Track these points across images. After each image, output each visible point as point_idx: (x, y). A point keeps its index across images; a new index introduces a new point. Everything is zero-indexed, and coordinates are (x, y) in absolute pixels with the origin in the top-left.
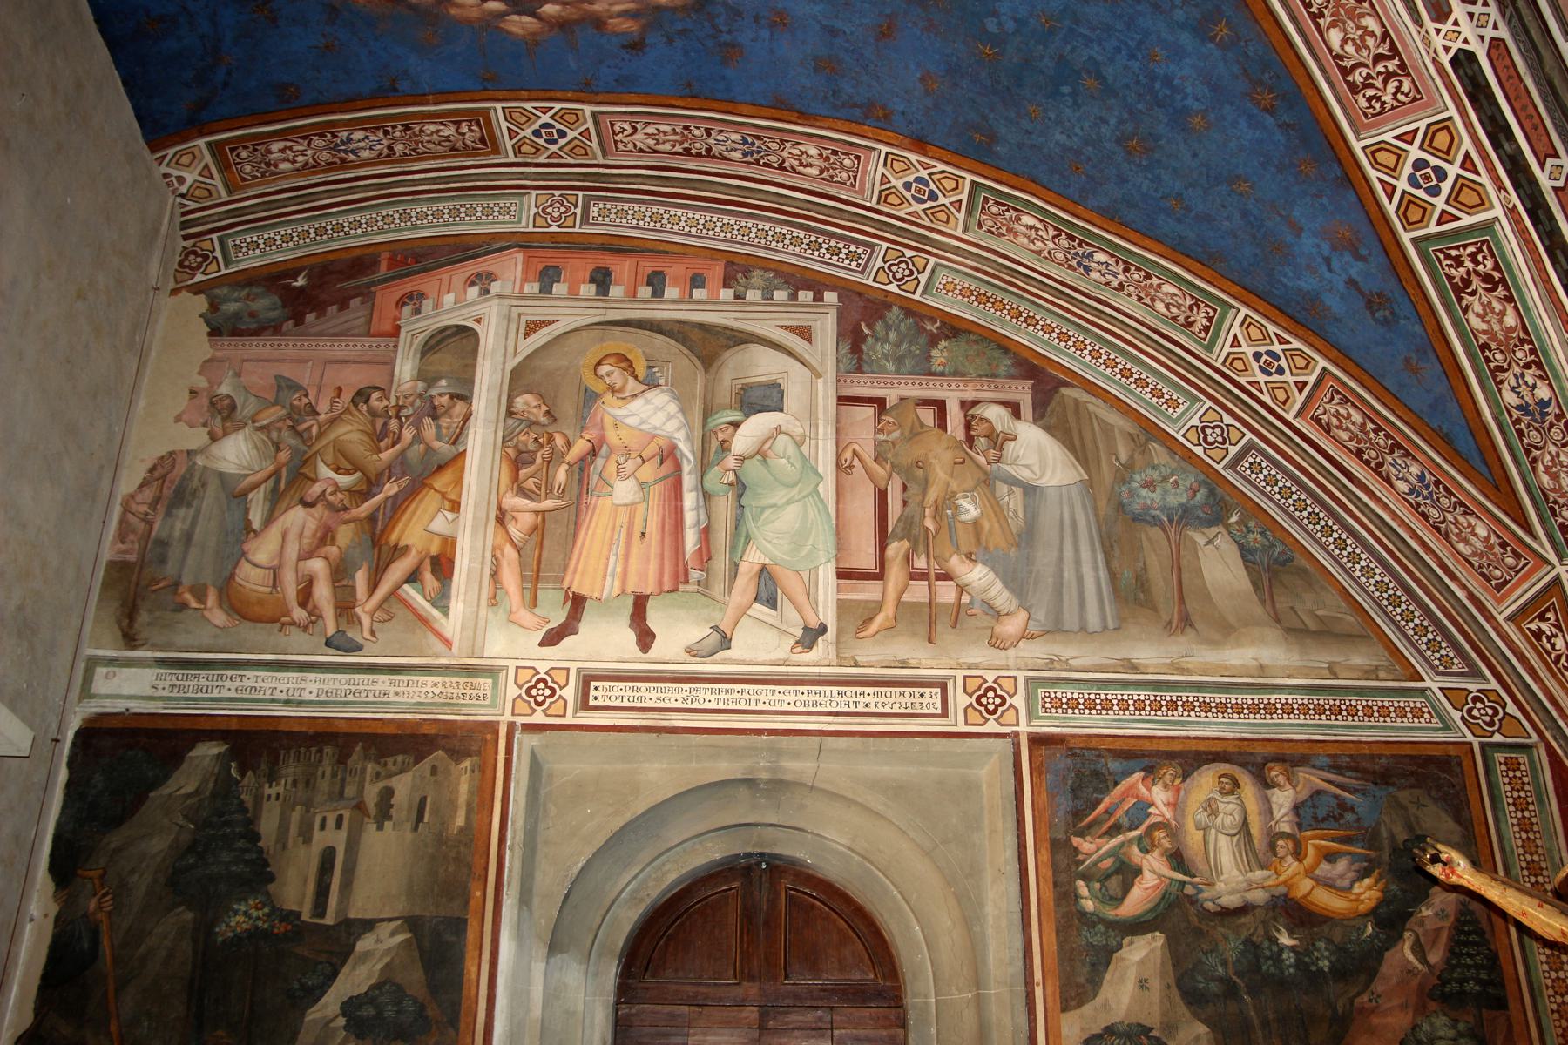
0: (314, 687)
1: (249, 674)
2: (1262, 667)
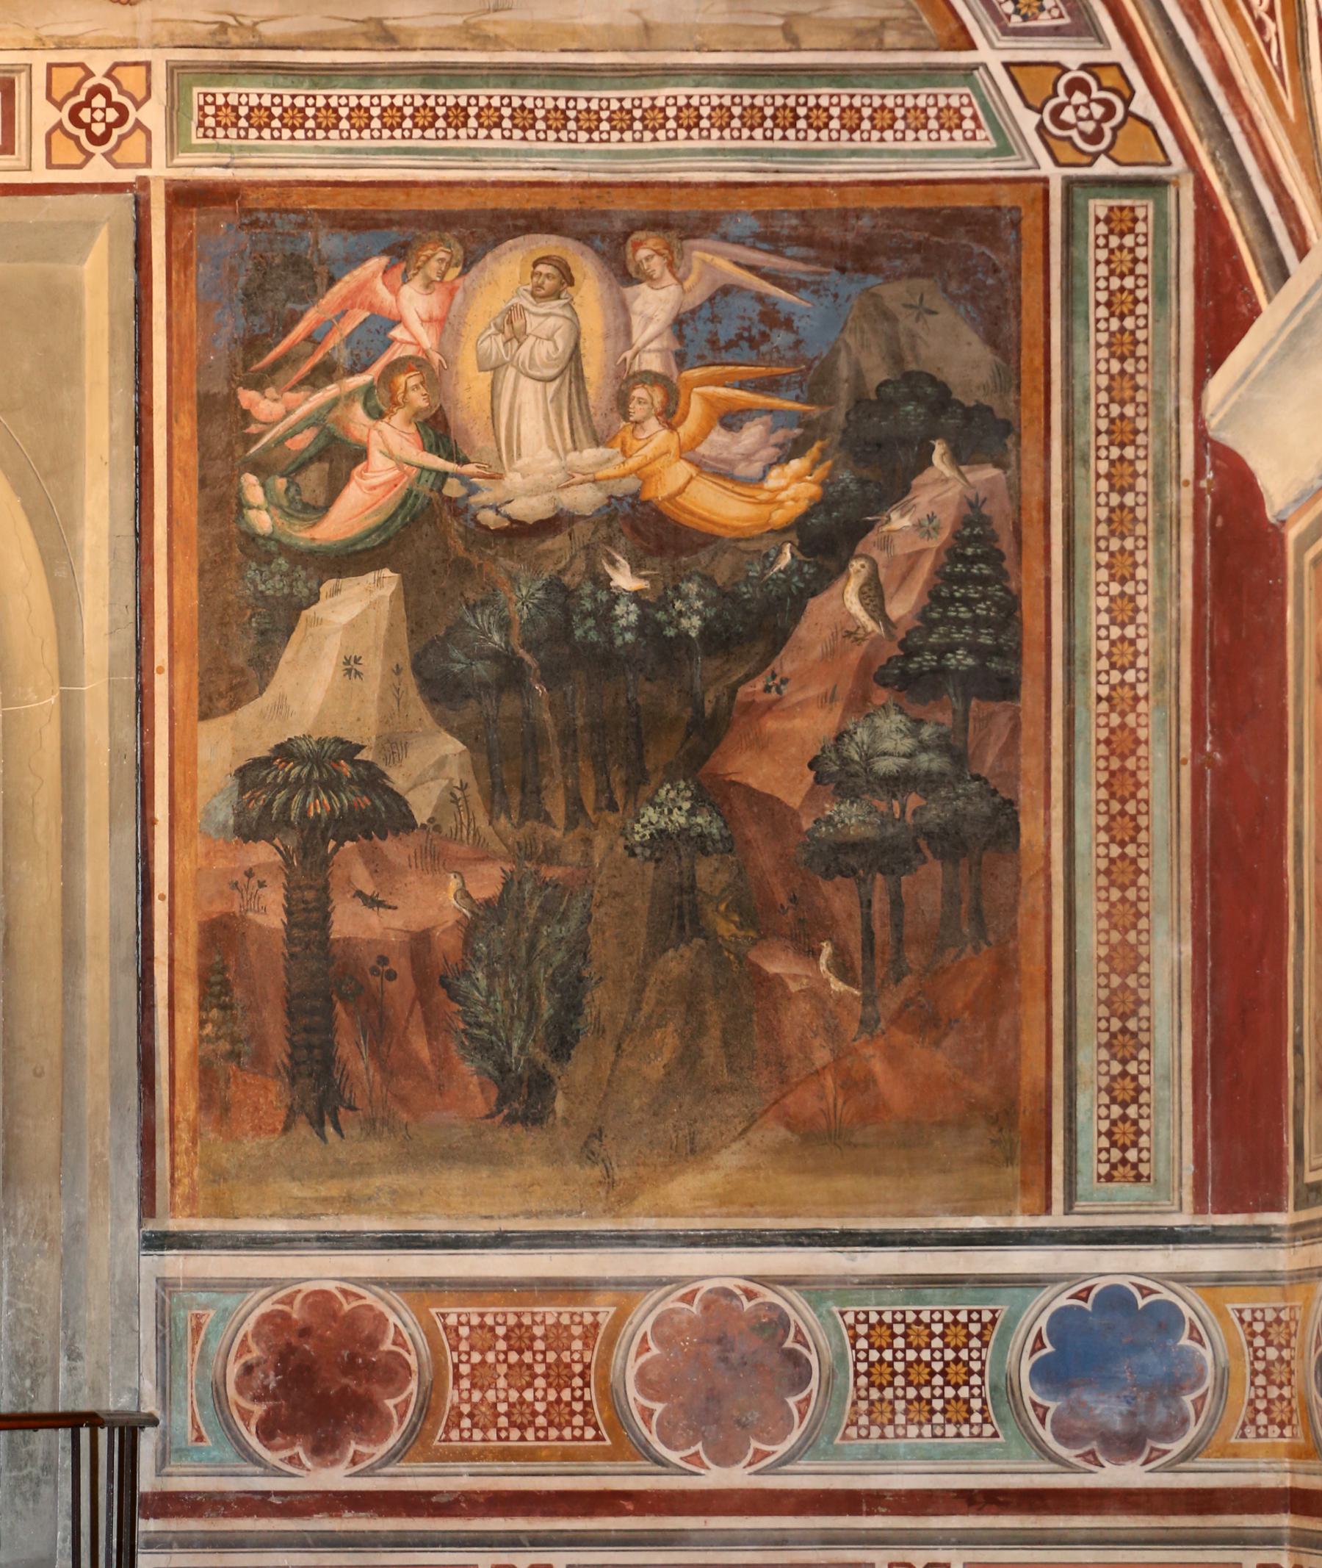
2: (647, 28)
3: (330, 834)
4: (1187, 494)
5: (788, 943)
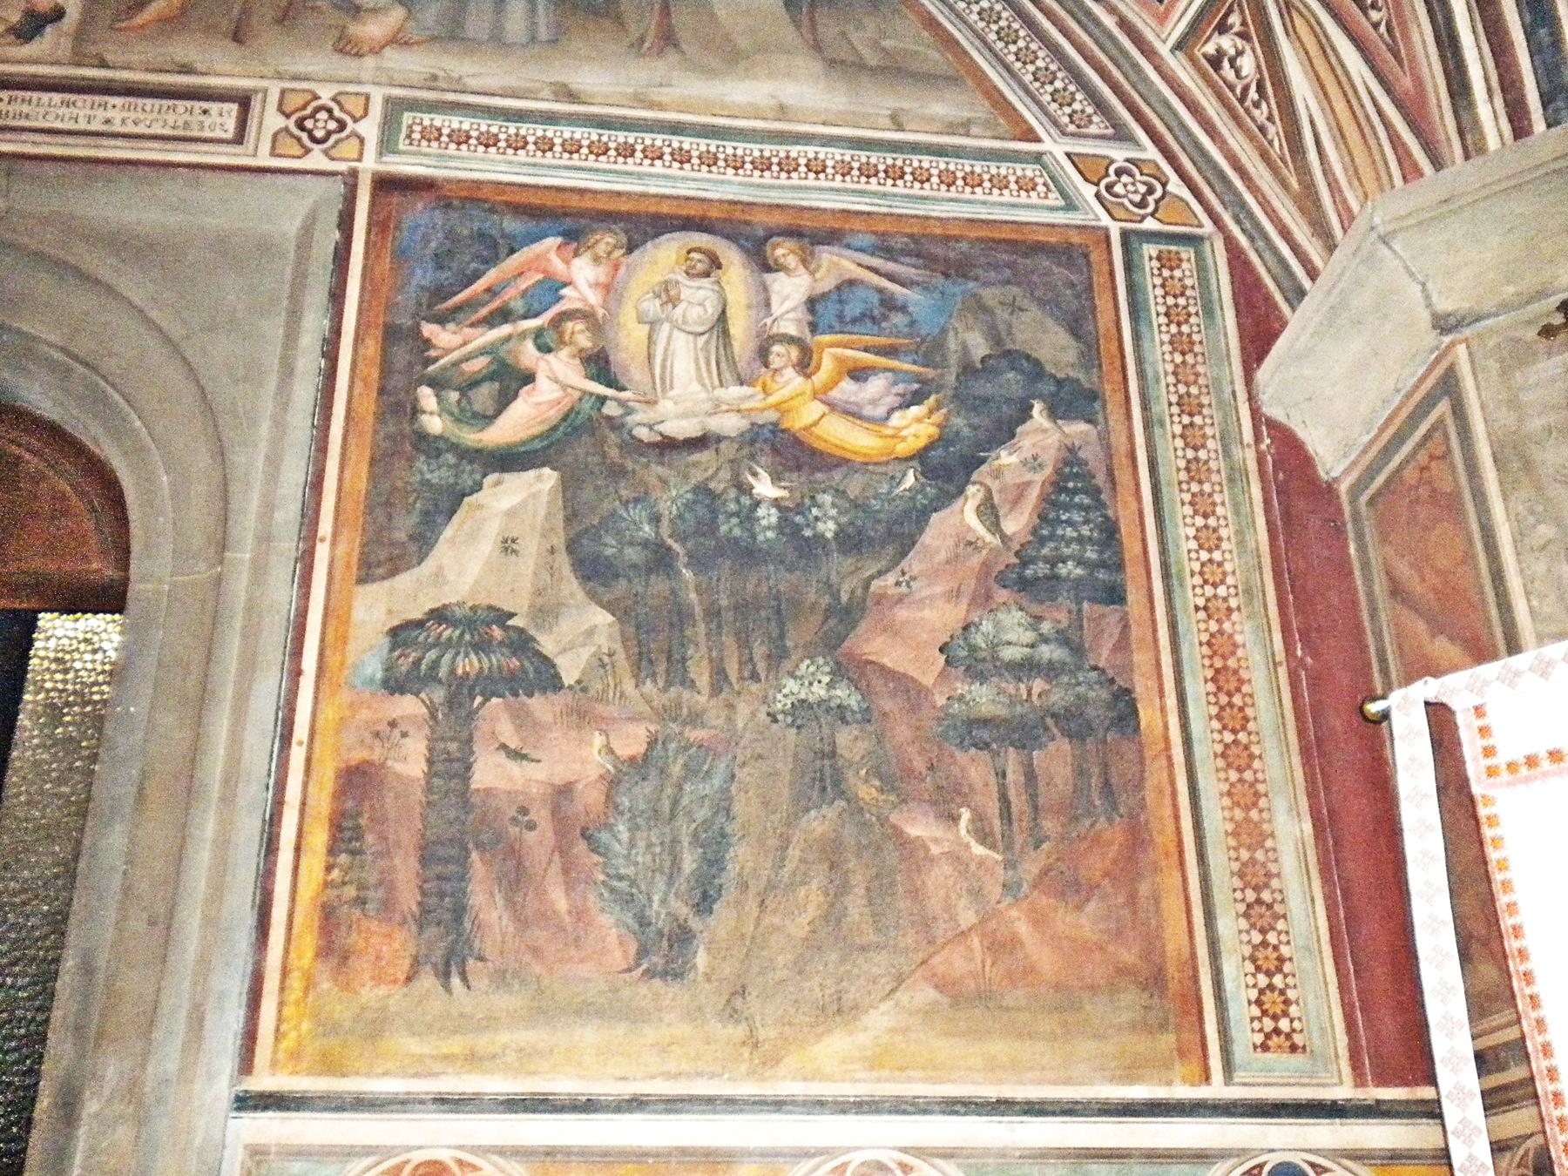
2: (782, 108)
3: (478, 689)
4: (1251, 456)
5: (926, 807)
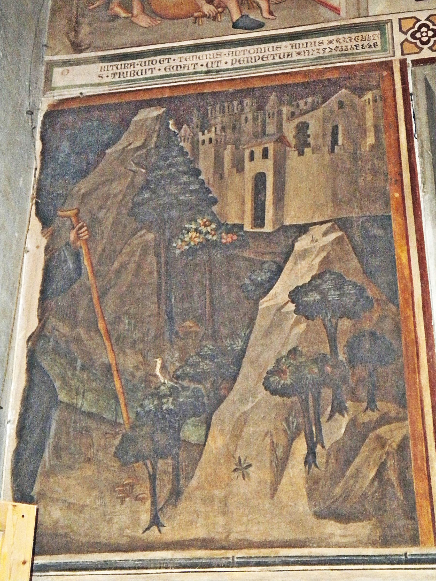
0: (229, 59)
1: (173, 57)
